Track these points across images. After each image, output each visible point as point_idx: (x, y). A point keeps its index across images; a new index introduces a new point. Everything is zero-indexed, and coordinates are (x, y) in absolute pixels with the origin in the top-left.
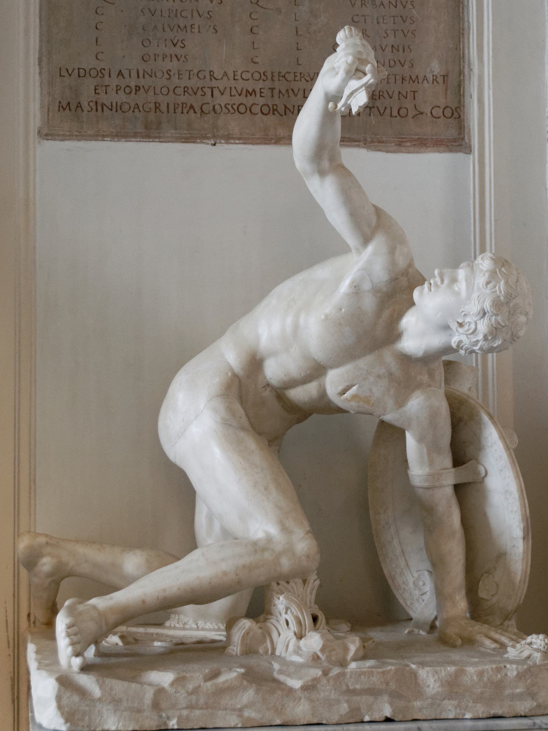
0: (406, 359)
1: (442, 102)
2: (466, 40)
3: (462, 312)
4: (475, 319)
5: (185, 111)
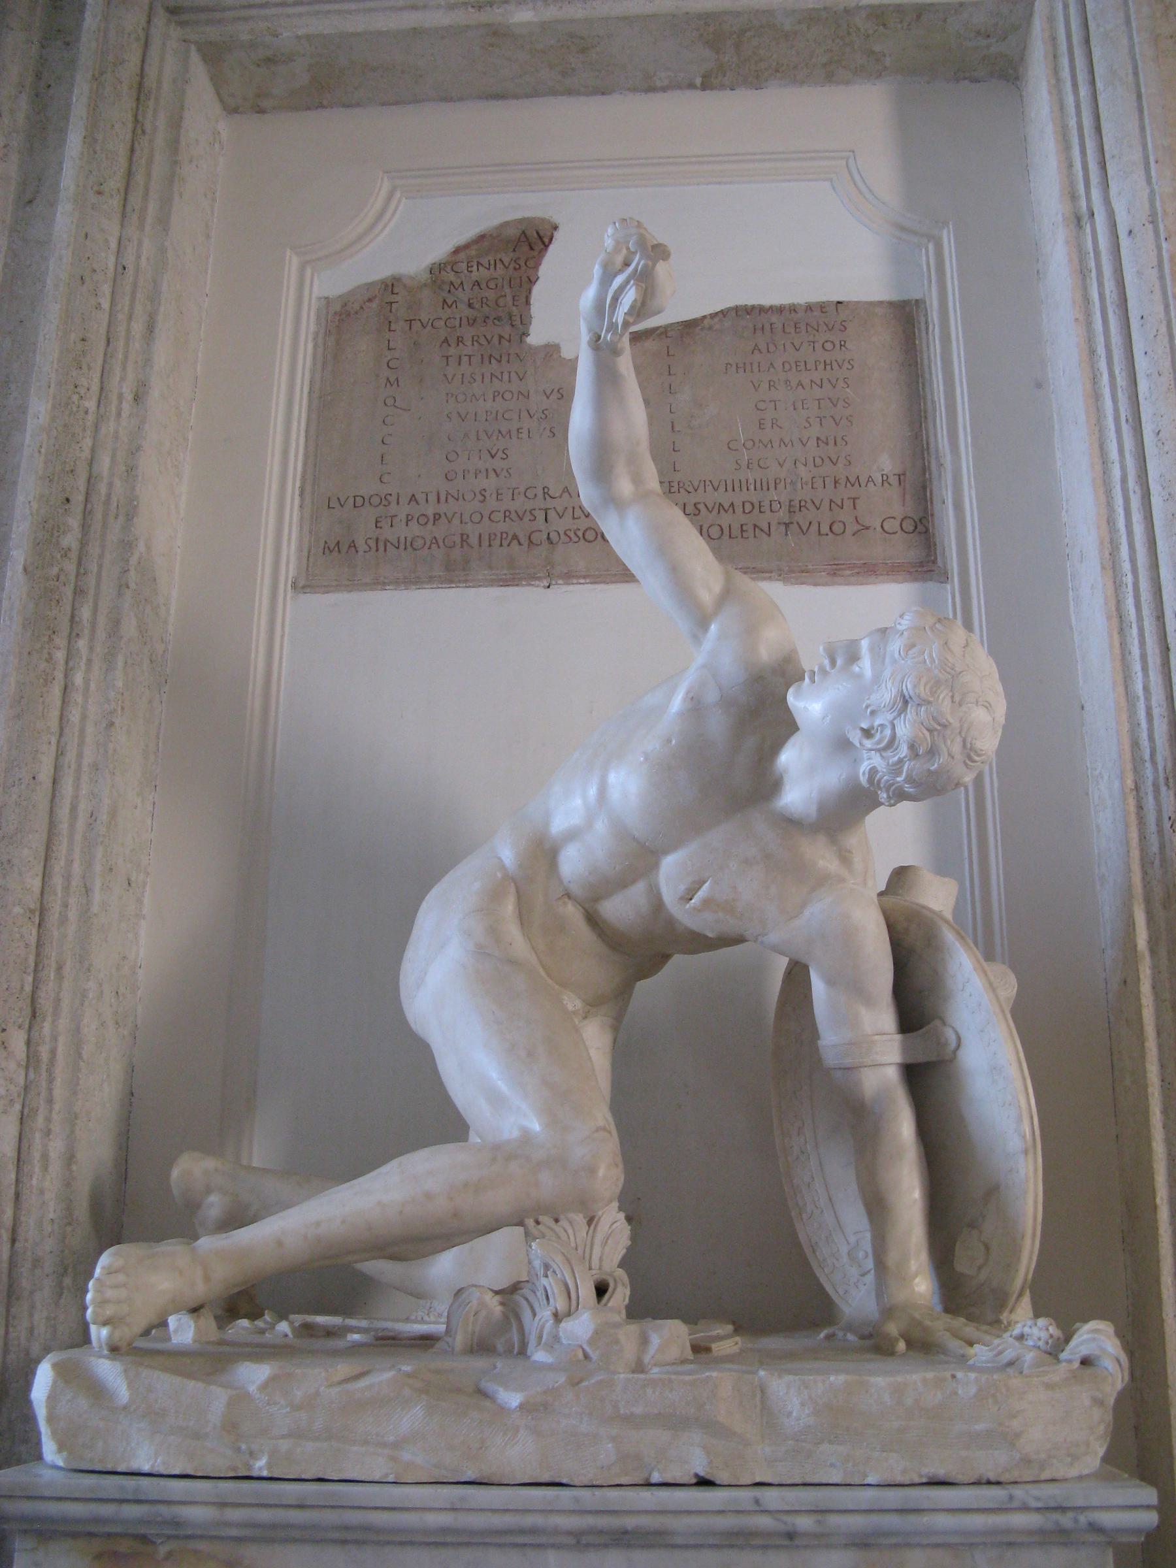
0: (790, 824)
1: (898, 510)
2: (931, 426)
3: (867, 707)
4: (890, 717)
5: (505, 543)
